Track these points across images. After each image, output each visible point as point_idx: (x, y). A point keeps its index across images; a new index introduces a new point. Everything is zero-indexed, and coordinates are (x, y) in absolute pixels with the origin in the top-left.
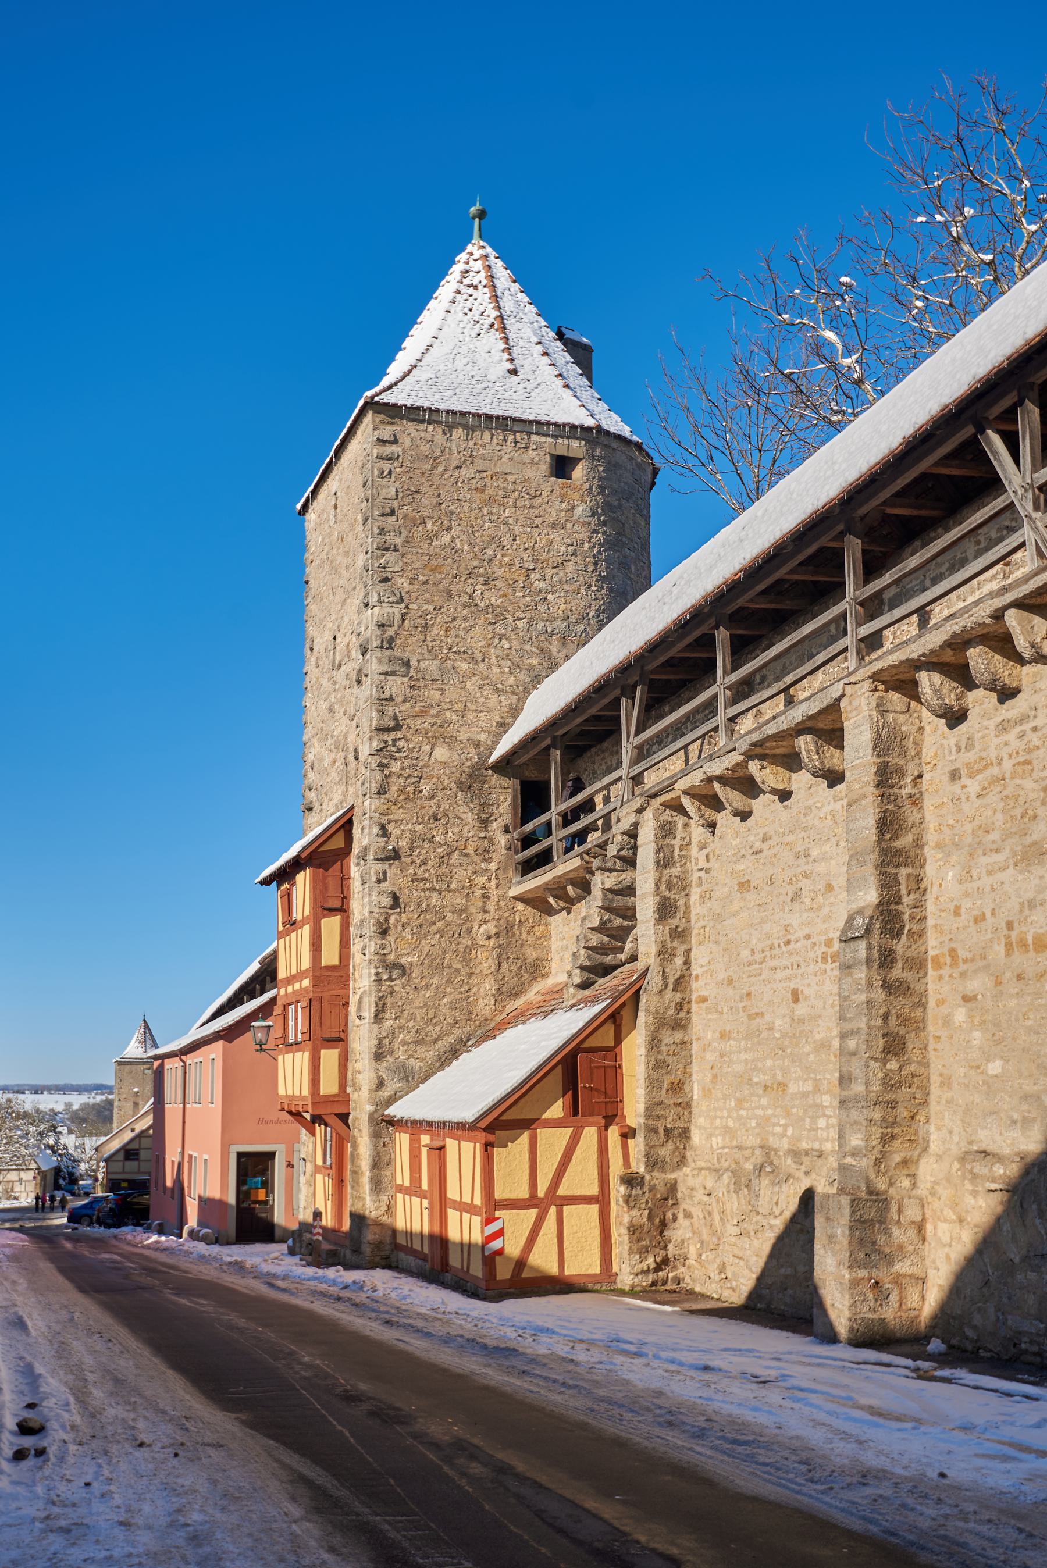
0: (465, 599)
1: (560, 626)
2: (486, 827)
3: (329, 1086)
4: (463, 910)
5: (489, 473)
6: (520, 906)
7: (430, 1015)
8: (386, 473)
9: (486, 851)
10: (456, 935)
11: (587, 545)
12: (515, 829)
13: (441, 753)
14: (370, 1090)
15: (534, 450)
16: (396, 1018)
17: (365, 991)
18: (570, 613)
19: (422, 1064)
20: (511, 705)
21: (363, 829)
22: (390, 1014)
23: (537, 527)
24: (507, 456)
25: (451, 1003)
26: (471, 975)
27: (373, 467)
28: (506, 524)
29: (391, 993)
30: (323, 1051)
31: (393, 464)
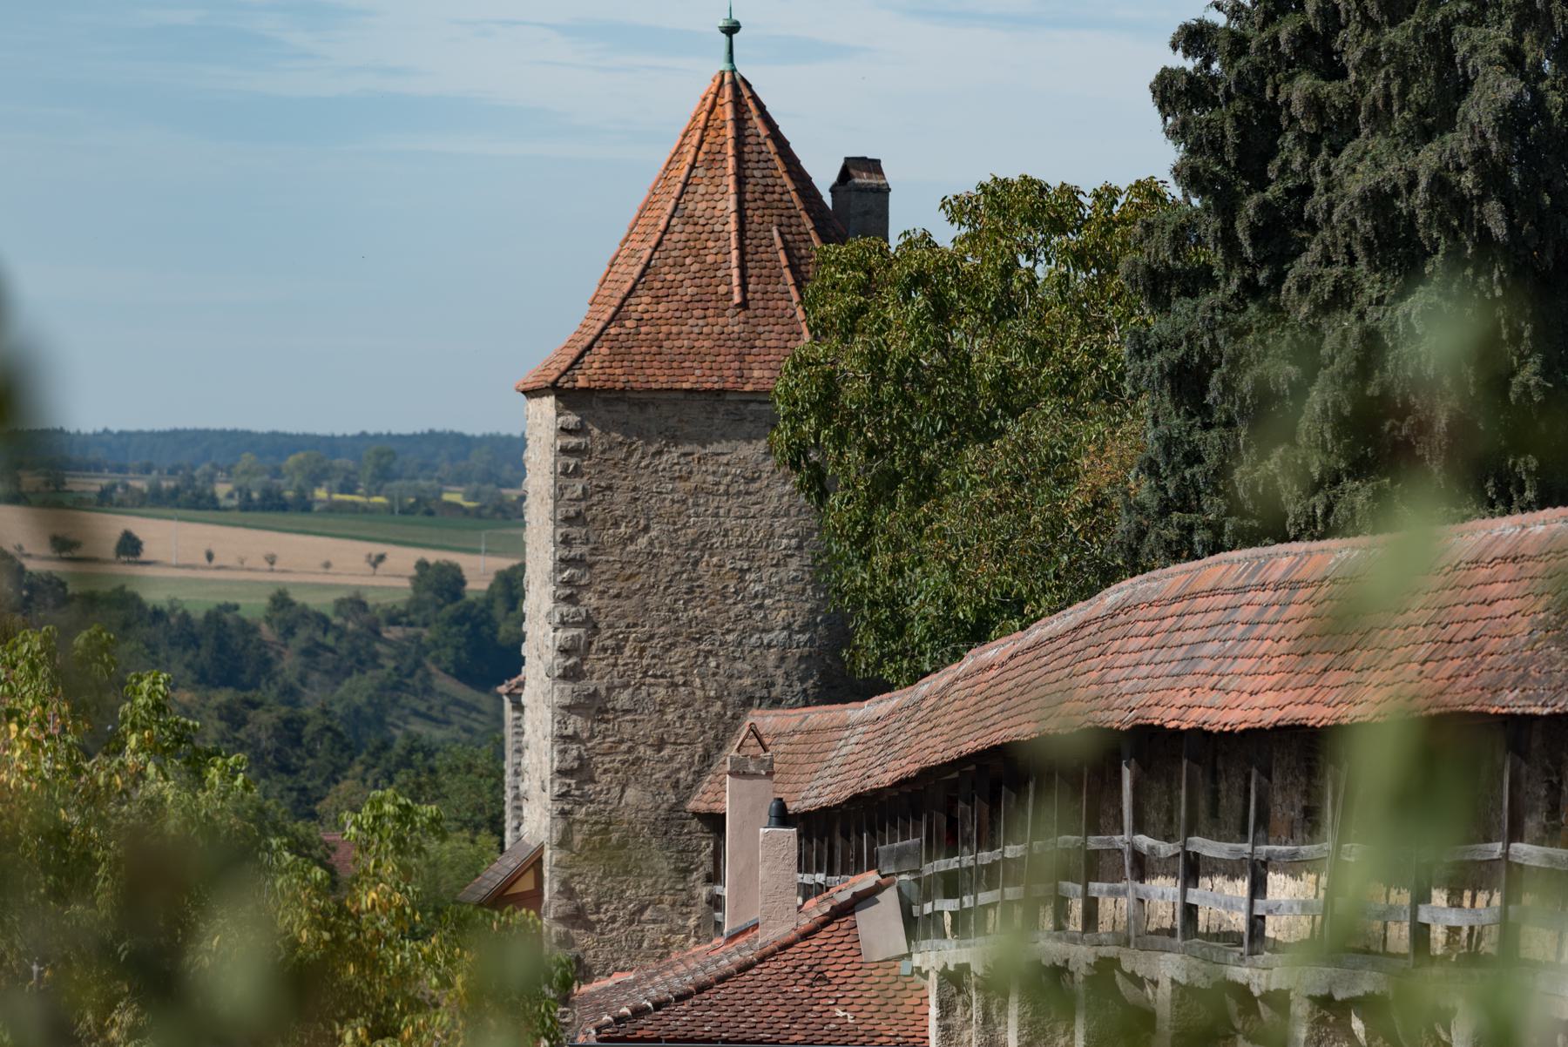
1: (779, 636)
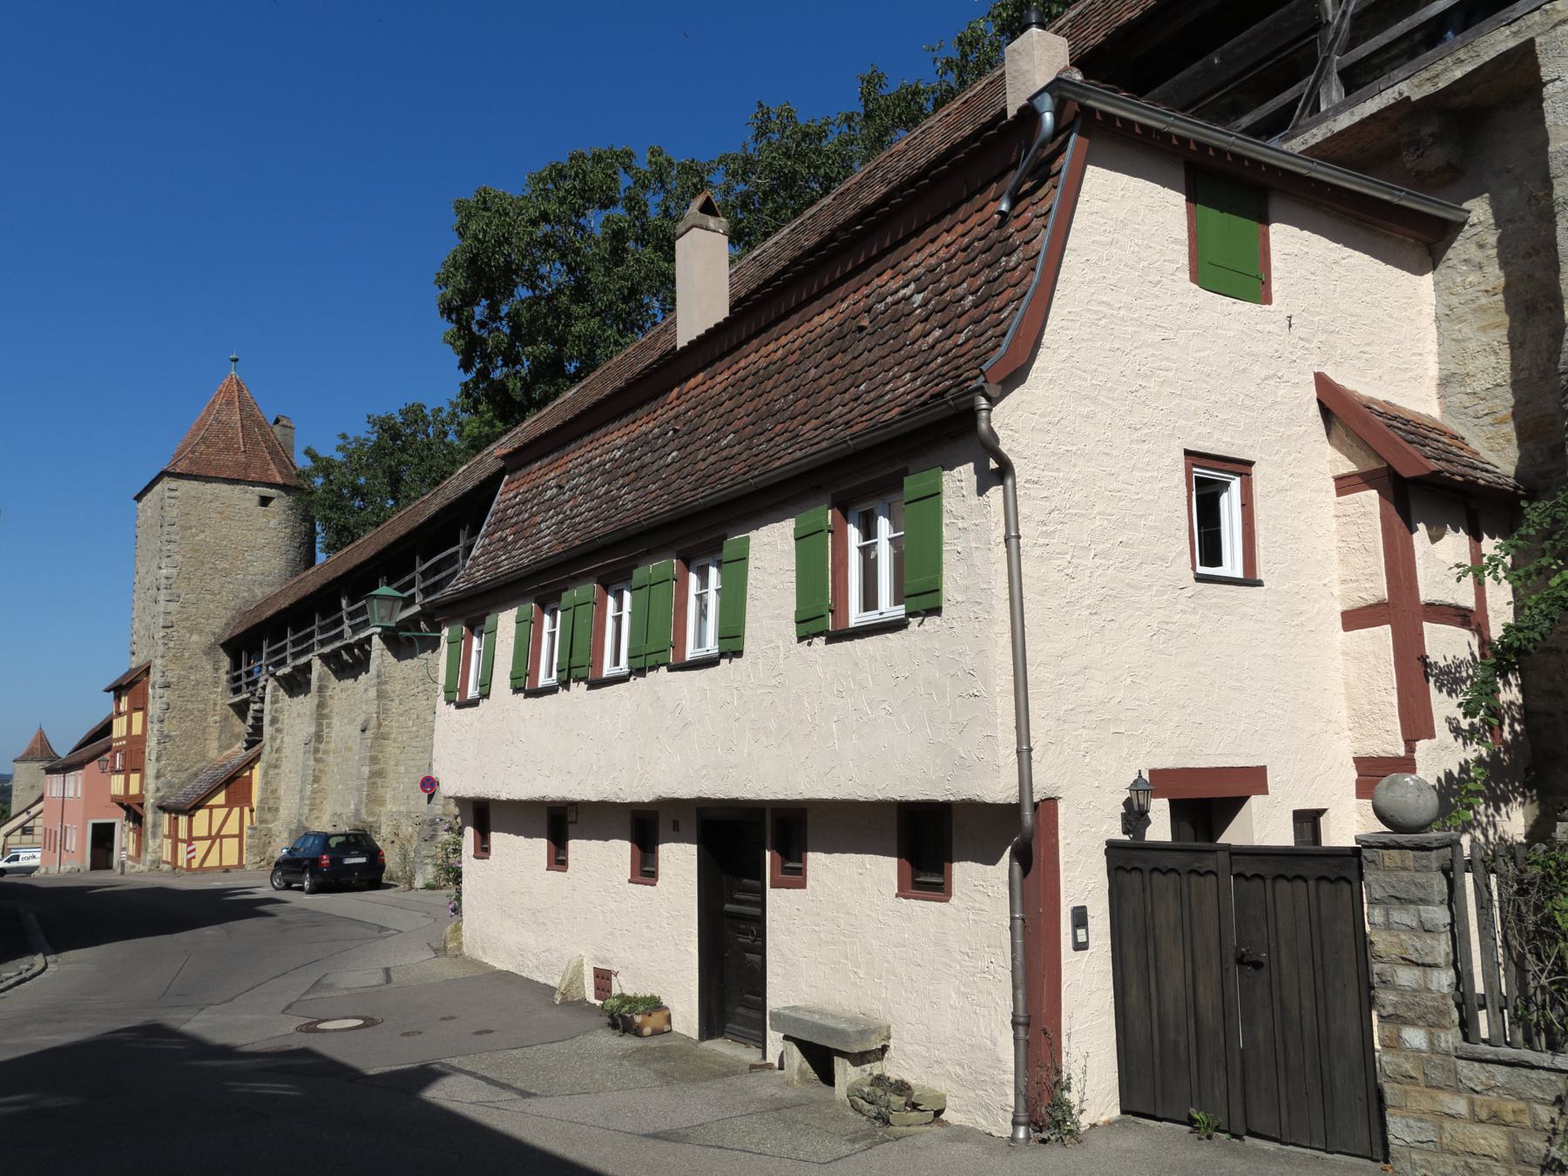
13: (195, 638)
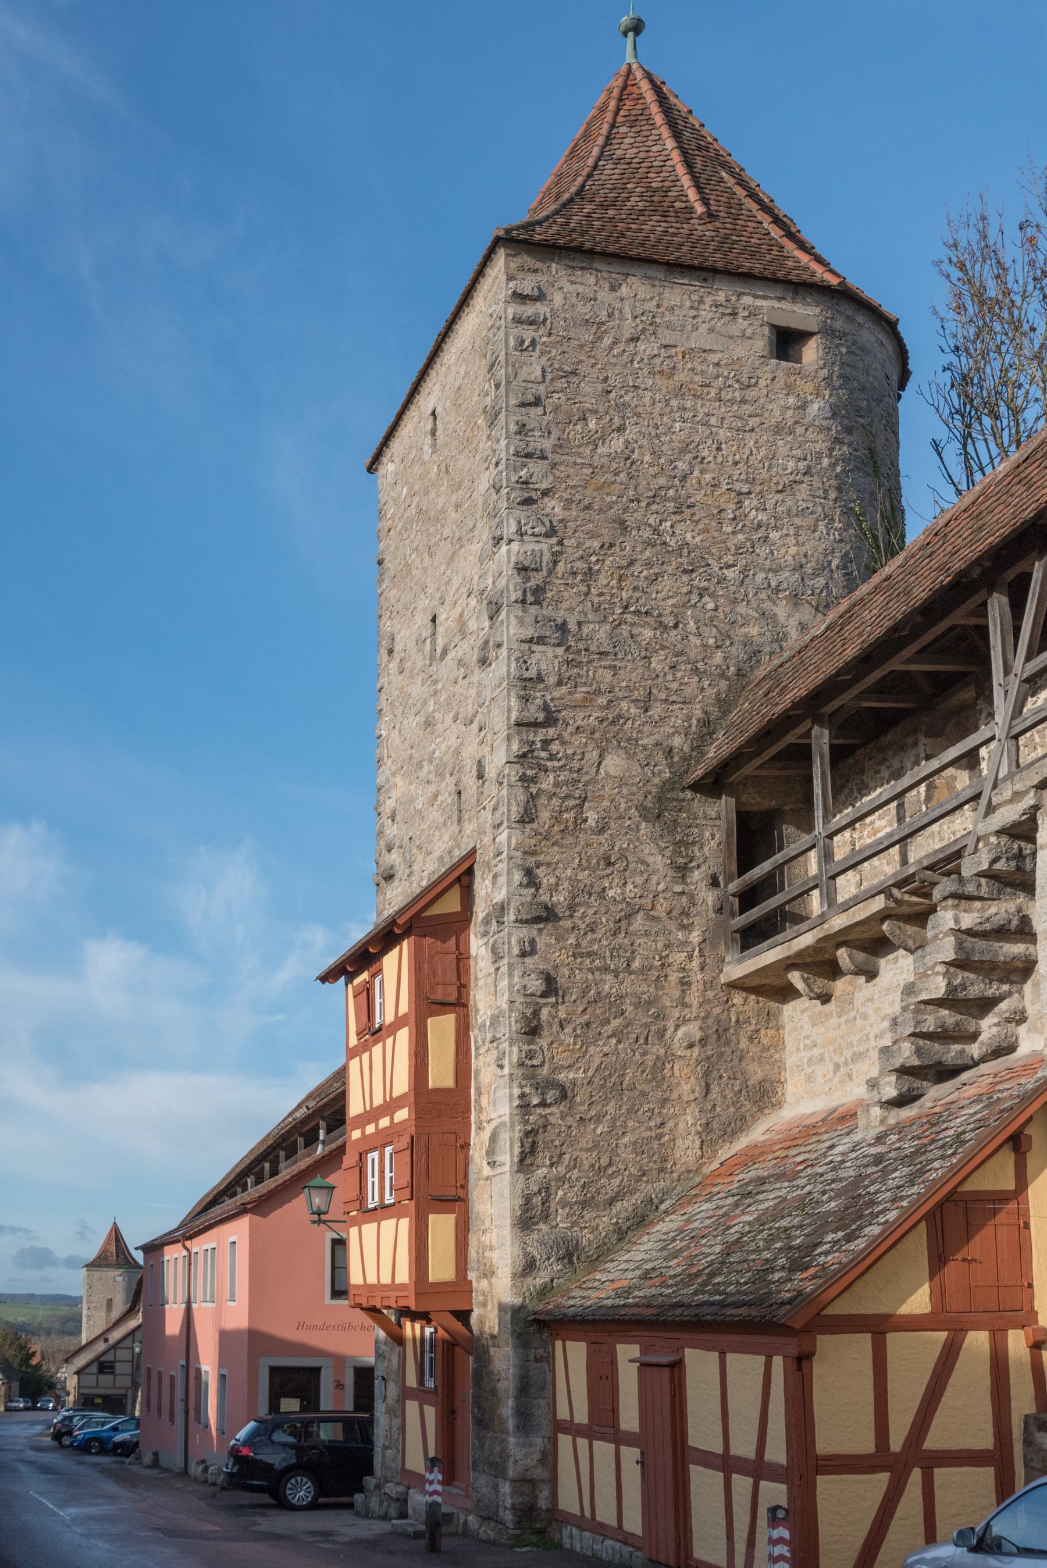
0: (646, 534)
2: (683, 877)
3: (441, 1268)
4: (650, 1003)
5: (679, 350)
6: (738, 998)
7: (604, 1161)
8: (527, 343)
9: (685, 913)
10: (641, 1041)
11: (826, 461)
12: (729, 879)
14: (514, 1275)
15: (745, 318)
16: (552, 1165)
17: (502, 1124)
18: (804, 560)
19: (591, 1237)
20: (718, 694)
21: (495, 876)
22: (543, 1158)
23: (752, 430)
24: (706, 326)
25: (635, 1143)
26: (664, 1101)
27: (507, 335)
28: (706, 424)
29: (545, 1127)
30: (431, 1217)
31: (536, 330)
